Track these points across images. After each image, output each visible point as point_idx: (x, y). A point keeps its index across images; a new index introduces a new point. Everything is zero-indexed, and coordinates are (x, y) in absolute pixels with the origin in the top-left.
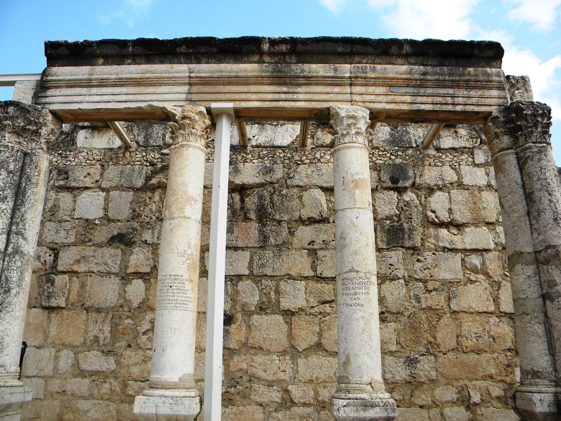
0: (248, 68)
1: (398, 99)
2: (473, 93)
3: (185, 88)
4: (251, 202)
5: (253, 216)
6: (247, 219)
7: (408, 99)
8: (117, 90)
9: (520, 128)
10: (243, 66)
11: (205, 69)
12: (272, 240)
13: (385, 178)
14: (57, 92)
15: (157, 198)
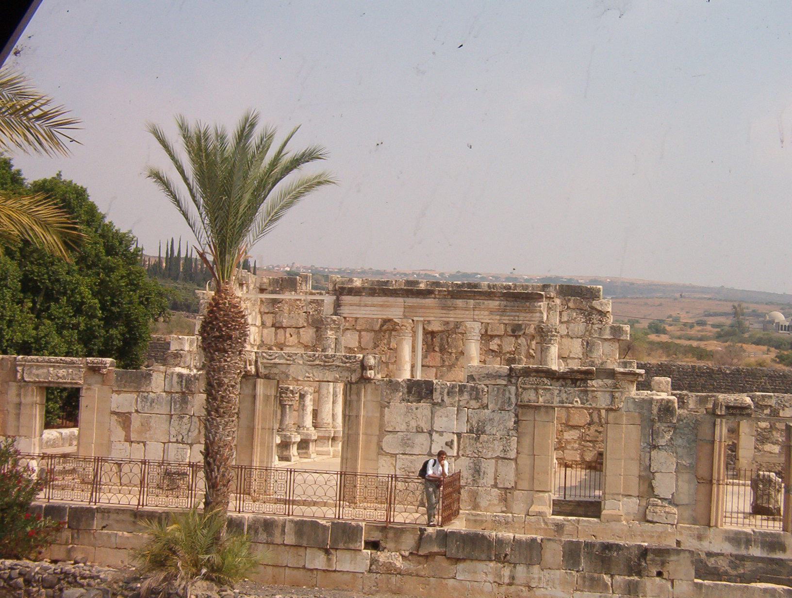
0: (429, 301)
1: (494, 317)
2: (527, 315)
3: (402, 310)
4: (437, 340)
5: (437, 349)
6: (434, 351)
7: (498, 317)
8: (373, 308)
9: (542, 336)
10: (427, 300)
11: (412, 301)
12: (447, 363)
13: (509, 329)
14: (346, 308)
15: (387, 336)
